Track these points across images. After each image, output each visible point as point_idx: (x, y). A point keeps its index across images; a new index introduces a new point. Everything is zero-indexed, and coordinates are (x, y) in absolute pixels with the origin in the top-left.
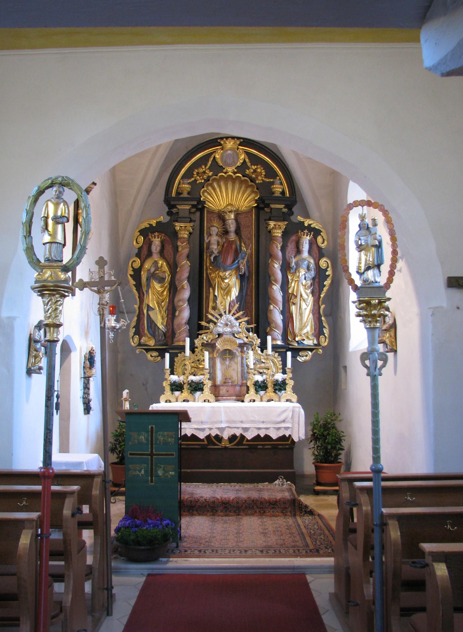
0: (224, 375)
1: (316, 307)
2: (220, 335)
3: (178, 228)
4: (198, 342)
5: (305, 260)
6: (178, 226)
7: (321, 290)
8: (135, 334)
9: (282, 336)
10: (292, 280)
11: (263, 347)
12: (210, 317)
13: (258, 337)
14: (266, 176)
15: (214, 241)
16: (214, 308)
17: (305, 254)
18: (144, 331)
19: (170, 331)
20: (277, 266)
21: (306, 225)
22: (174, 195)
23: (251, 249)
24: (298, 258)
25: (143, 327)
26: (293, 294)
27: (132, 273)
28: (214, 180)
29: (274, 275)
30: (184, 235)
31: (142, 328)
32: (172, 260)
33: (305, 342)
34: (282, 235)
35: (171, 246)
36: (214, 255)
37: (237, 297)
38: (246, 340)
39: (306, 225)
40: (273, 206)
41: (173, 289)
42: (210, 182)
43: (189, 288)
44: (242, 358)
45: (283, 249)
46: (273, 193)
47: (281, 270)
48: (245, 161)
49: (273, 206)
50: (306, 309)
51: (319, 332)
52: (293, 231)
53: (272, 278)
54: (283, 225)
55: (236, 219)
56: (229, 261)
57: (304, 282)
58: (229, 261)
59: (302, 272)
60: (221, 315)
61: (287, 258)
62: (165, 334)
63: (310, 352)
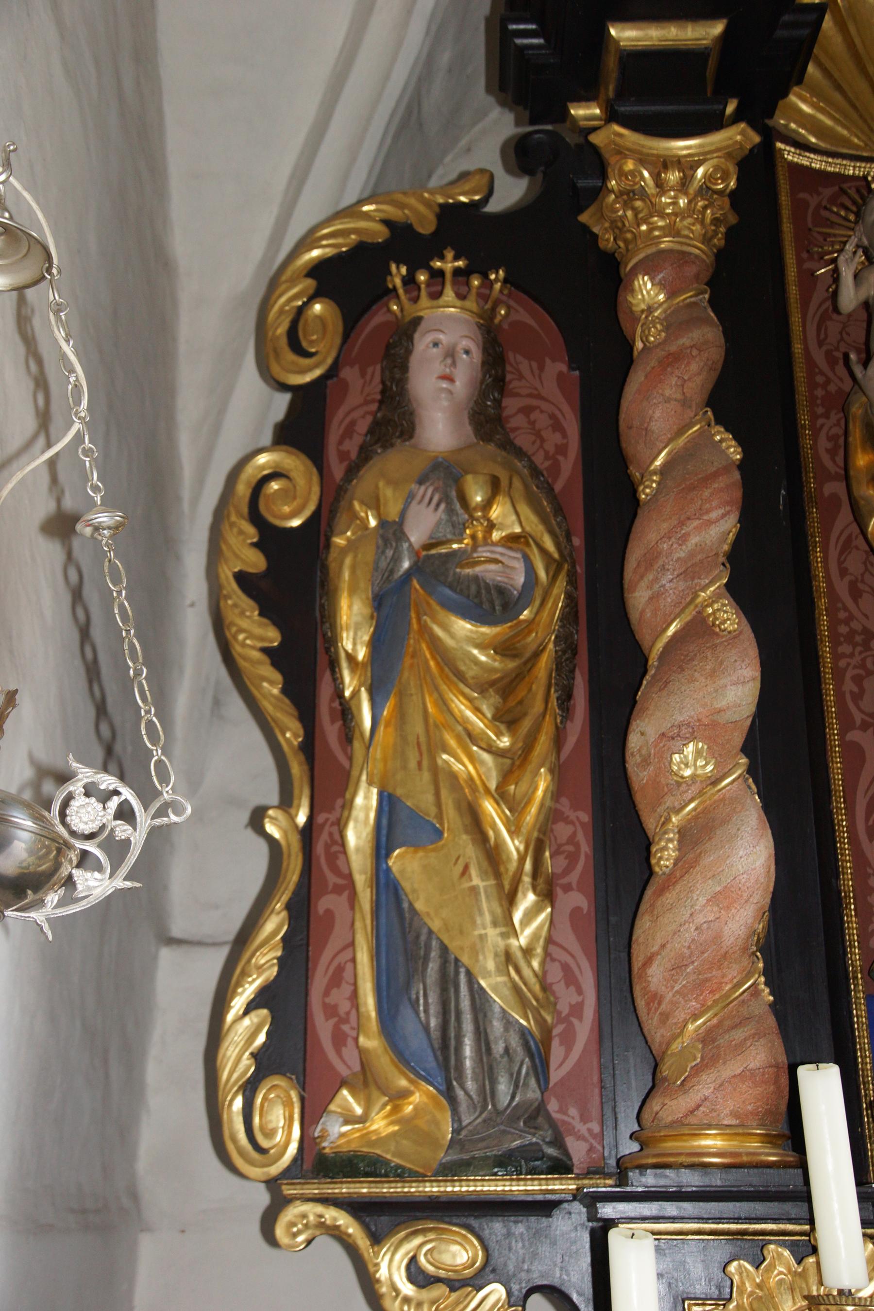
8: (266, 1063)
25: (340, 997)
27: (255, 562)
31: (331, 1011)
41: (606, 668)
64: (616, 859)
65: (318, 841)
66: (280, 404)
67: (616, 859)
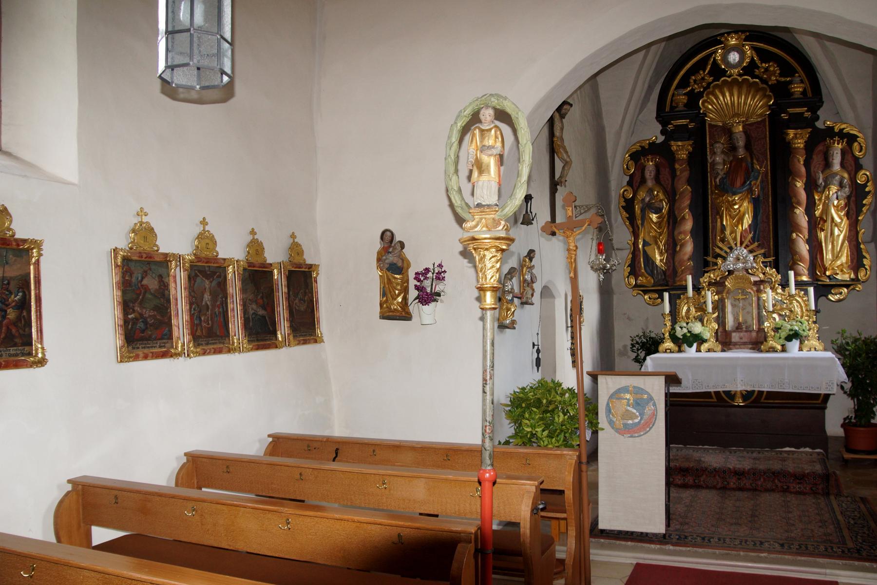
0: (736, 318)
1: (853, 233)
2: (730, 272)
3: (674, 148)
4: (704, 280)
5: (836, 174)
6: (675, 145)
7: (859, 212)
8: (630, 274)
9: (808, 270)
10: (820, 200)
11: (785, 285)
12: (718, 250)
13: (778, 272)
14: (781, 75)
15: (718, 159)
16: (723, 240)
17: (837, 167)
18: (640, 271)
19: (671, 268)
20: (800, 184)
21: (836, 130)
22: (667, 109)
23: (766, 167)
24: (828, 171)
26: (821, 218)
27: (624, 204)
28: (717, 86)
29: (795, 196)
30: (683, 155)
32: (669, 186)
33: (839, 277)
34: (805, 146)
35: (667, 170)
36: (720, 177)
37: (750, 226)
38: (761, 276)
39: (836, 130)
40: (791, 110)
41: (673, 221)
42: (711, 89)
43: (691, 217)
44: (759, 299)
45: (807, 164)
46: (792, 94)
47: (804, 189)
48: (752, 59)
49: (791, 110)
50: (839, 236)
51: (857, 263)
52: (820, 138)
53: (794, 200)
54: (806, 133)
55: (745, 131)
56: (738, 183)
57: (836, 202)
58: (738, 183)
59: (834, 189)
60: (731, 248)
61: (813, 174)
62: (664, 272)
63: (846, 290)
64: (672, 247)
65: (635, 244)
66: (628, 178)
67: (672, 247)
